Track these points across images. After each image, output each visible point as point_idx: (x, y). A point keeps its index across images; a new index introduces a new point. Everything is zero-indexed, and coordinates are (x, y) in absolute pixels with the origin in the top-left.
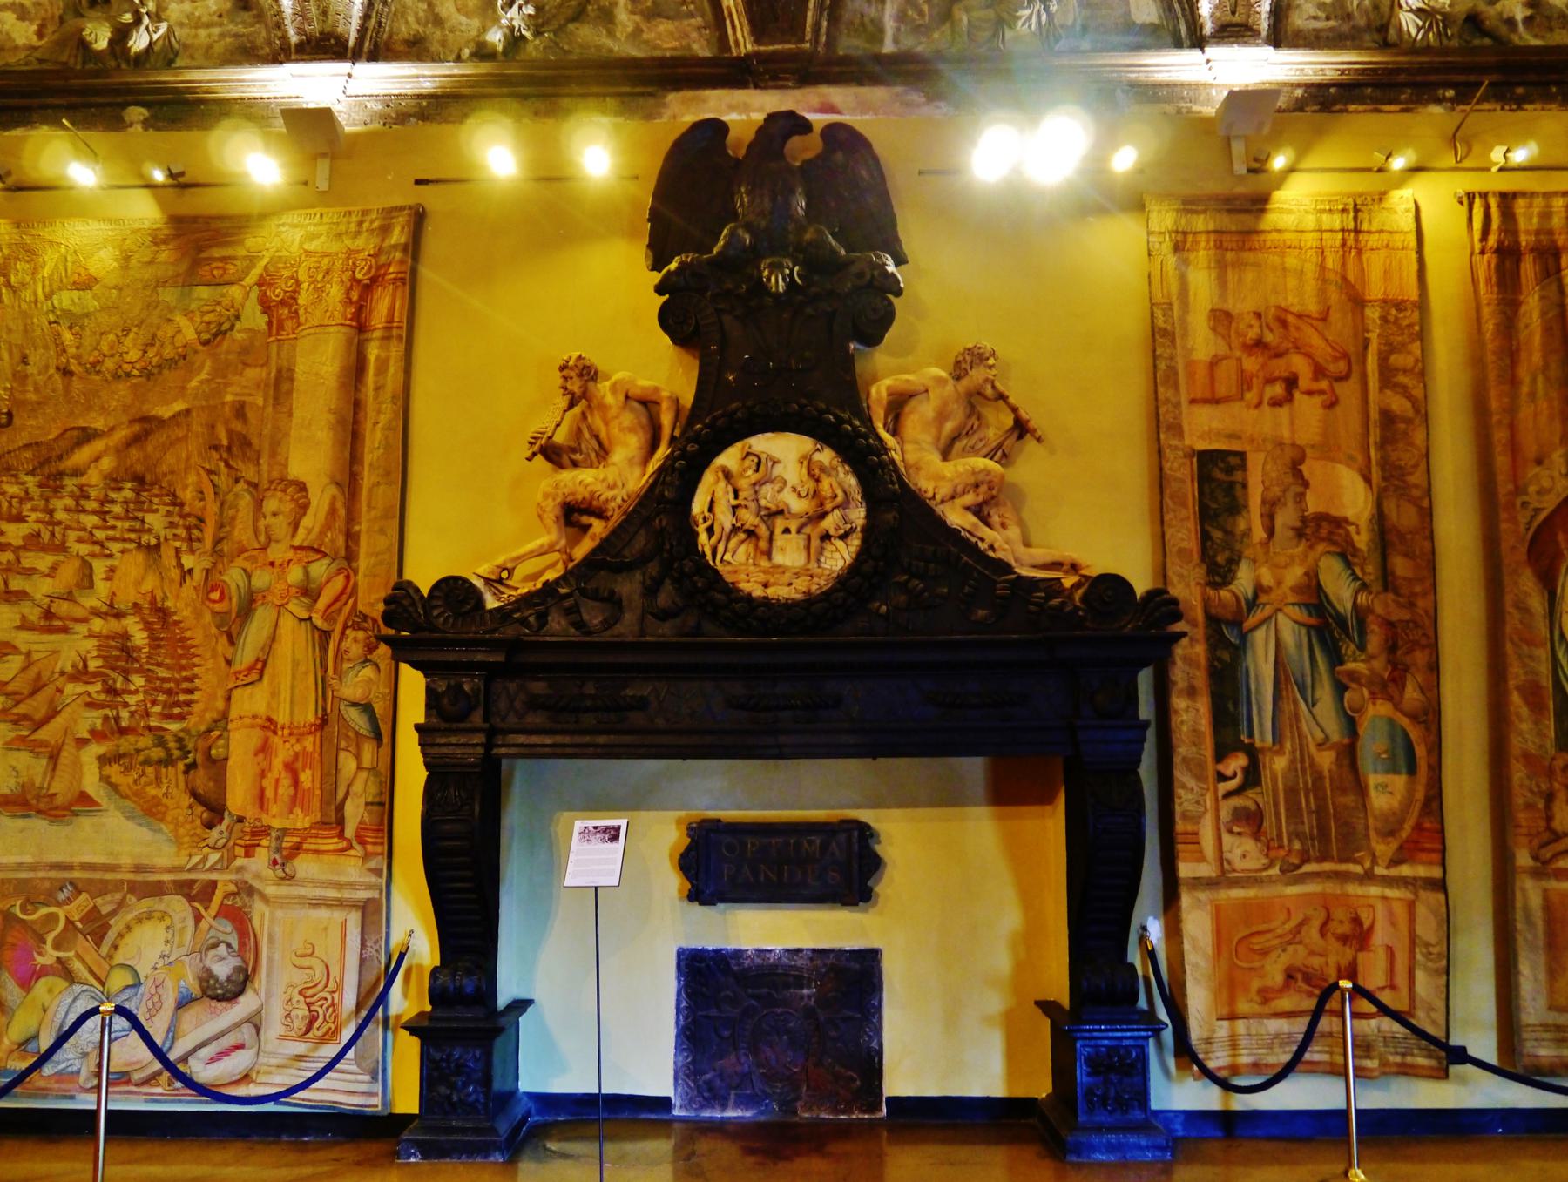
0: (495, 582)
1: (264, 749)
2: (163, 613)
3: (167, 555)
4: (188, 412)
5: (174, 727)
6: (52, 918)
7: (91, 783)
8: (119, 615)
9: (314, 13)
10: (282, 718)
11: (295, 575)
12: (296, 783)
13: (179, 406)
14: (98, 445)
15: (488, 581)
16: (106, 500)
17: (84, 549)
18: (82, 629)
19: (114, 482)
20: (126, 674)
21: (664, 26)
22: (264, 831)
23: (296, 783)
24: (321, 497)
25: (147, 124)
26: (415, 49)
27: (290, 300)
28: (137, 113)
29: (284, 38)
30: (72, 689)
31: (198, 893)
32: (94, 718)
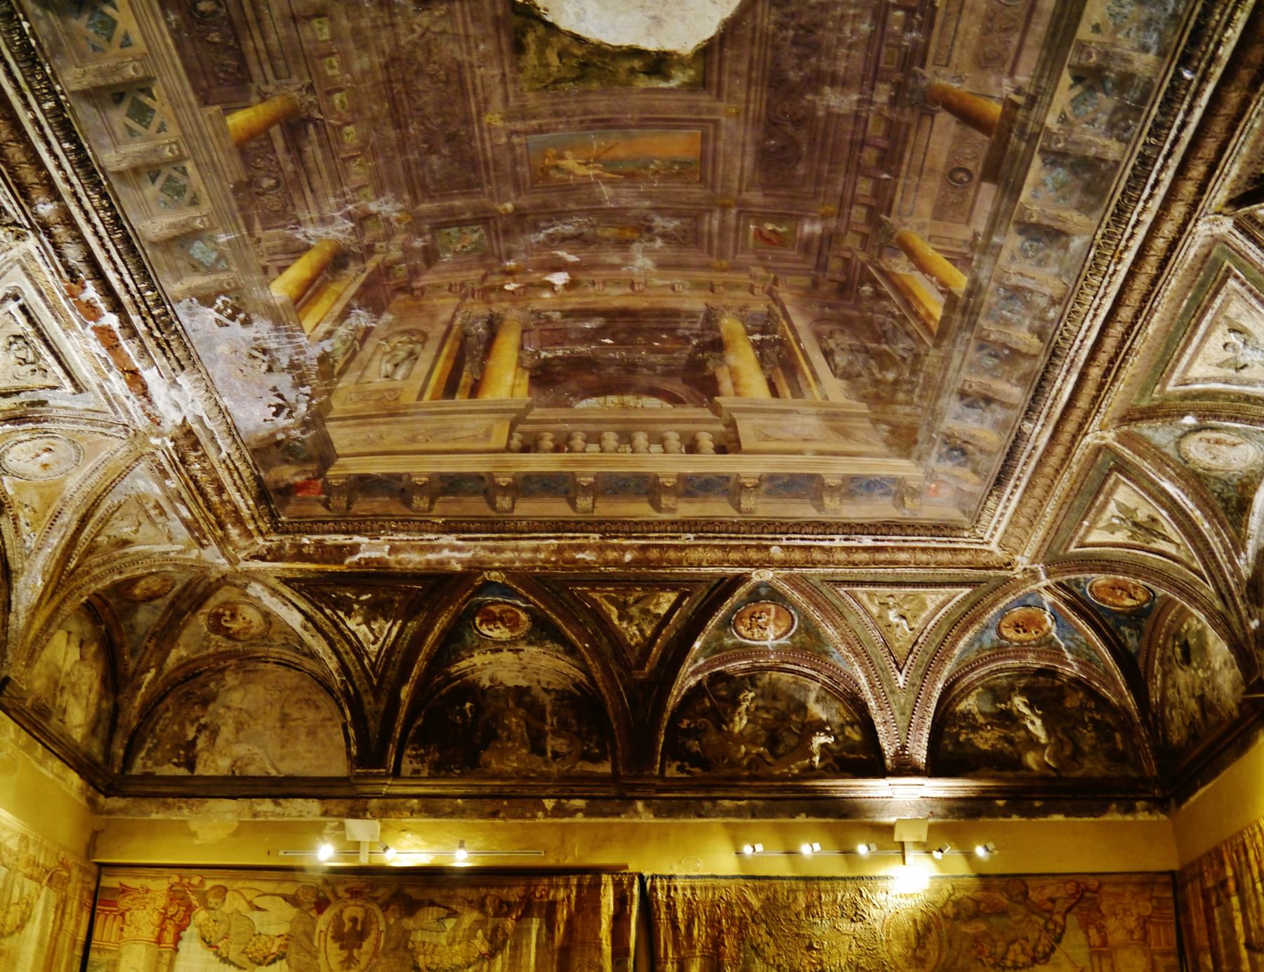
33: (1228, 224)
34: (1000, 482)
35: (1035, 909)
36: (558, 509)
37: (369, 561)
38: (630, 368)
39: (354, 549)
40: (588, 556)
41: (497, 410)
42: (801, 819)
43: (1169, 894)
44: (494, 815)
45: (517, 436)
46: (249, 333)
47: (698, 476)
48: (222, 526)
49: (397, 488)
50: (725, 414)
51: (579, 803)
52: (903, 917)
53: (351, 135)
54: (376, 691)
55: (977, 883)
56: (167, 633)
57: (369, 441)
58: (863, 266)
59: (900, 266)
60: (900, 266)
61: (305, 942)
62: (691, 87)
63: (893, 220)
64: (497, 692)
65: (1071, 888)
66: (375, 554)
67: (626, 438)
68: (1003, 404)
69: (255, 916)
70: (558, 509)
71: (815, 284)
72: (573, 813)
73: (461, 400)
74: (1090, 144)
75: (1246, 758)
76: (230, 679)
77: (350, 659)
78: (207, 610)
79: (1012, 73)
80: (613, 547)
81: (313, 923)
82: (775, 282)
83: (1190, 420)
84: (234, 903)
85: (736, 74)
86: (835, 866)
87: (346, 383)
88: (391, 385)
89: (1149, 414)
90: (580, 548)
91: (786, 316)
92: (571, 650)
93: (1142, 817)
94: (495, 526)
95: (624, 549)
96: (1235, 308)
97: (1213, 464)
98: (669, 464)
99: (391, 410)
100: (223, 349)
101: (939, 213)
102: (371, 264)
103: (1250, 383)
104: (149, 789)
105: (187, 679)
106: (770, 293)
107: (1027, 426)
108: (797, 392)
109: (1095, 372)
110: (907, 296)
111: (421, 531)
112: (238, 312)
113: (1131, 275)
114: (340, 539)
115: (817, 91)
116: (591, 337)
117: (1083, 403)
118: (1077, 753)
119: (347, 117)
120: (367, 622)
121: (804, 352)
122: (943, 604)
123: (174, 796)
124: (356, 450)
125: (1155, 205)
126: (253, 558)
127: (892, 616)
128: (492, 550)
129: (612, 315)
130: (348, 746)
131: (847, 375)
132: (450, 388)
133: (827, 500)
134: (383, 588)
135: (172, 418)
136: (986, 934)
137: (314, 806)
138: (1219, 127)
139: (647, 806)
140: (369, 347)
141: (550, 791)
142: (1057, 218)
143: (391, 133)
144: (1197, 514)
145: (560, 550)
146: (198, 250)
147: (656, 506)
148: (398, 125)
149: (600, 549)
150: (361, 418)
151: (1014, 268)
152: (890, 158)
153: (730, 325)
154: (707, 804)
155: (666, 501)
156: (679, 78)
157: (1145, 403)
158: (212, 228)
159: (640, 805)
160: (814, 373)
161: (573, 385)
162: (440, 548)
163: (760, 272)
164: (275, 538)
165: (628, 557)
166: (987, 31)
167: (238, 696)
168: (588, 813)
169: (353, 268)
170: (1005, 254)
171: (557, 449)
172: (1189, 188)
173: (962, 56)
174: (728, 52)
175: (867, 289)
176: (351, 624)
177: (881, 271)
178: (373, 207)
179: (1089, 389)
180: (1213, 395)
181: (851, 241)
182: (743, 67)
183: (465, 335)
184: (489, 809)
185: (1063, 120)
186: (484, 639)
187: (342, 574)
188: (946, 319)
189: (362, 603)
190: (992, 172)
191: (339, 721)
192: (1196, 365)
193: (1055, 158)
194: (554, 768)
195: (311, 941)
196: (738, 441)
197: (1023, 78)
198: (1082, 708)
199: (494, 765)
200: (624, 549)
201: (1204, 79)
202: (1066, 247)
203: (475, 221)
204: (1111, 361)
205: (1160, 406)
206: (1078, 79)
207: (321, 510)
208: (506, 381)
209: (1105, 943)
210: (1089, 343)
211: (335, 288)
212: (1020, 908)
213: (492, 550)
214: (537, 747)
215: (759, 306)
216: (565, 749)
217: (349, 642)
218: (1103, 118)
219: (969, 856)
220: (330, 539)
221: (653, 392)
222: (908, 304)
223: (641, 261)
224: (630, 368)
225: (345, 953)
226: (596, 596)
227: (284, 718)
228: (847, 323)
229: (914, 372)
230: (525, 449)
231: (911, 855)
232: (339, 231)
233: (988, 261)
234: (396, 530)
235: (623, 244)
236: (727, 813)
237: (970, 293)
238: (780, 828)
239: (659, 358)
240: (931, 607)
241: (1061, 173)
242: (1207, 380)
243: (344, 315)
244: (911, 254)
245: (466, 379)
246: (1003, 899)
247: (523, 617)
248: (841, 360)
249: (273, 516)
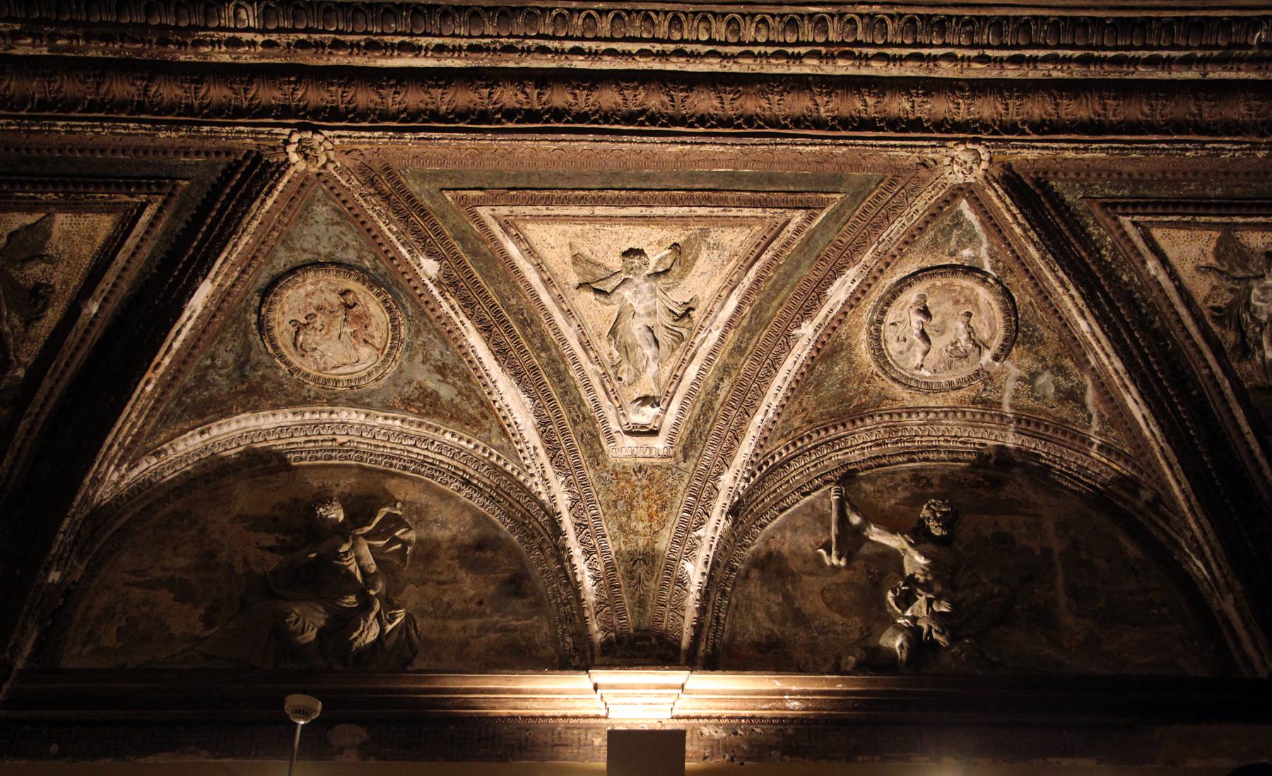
25: (365, 751)
29: (582, 634)
96: (735, 239)
117: (394, 100)
125: (978, 71)
157: (414, 187)
192: (558, 228)
204: (558, 114)
205: (423, 212)
242: (530, 252)
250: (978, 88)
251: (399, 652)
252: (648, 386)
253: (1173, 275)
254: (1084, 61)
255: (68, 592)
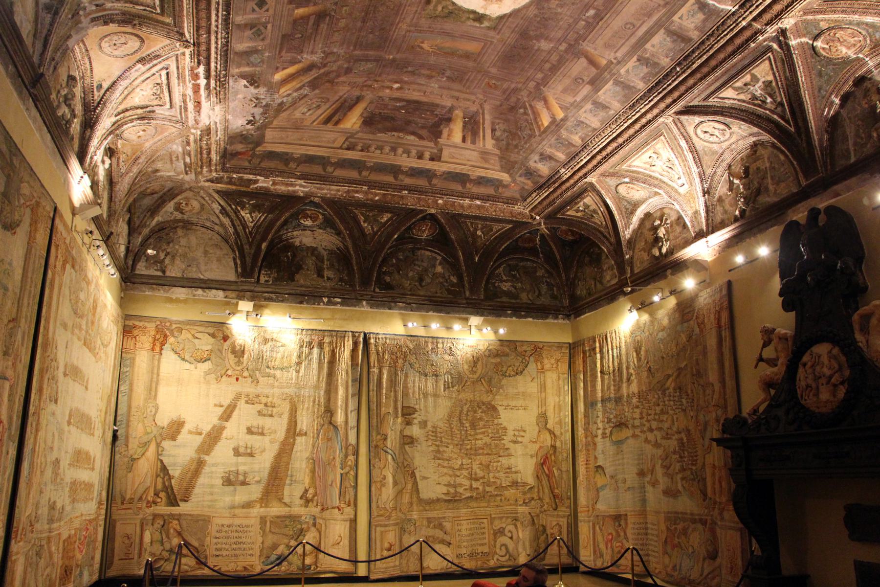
0: (755, 411)
1: (713, 475)
2: (688, 431)
3: (688, 411)
4: (686, 365)
5: (694, 468)
6: (676, 529)
7: (680, 487)
8: (680, 433)
9: (696, 223)
10: (716, 464)
11: (714, 415)
12: (721, 486)
13: (685, 363)
14: (671, 379)
15: (749, 414)
16: (674, 396)
17: (671, 412)
18: (674, 438)
19: (674, 389)
20: (683, 451)
21: (783, 185)
22: (715, 503)
23: (721, 486)
24: (717, 386)
25: (672, 274)
26: (722, 225)
27: (703, 322)
28: (669, 271)
30: (674, 457)
31: (704, 523)
32: (678, 466)
33: (671, 119)
34: (540, 187)
35: (519, 354)
36: (354, 174)
37: (261, 188)
38: (408, 123)
39: (256, 182)
40: (360, 196)
41: (343, 132)
42: (431, 313)
43: (568, 351)
44: (301, 303)
45: (347, 143)
46: (256, 91)
47: (418, 168)
48: (202, 167)
49: (285, 158)
50: (439, 146)
51: (339, 300)
52: (469, 355)
53: (342, 23)
54: (250, 244)
55: (498, 343)
56: (154, 210)
57: (282, 138)
58: (524, 102)
59: (539, 106)
60: (539, 106)
61: (219, 354)
62: (489, 28)
63: (545, 89)
64: (302, 248)
65: (532, 347)
66: (265, 185)
67: (394, 149)
68: (556, 161)
69: (196, 341)
70: (354, 174)
71: (501, 105)
72: (336, 304)
73: (329, 126)
74: (633, 81)
75: (611, 305)
76: (180, 232)
77: (240, 228)
78: (175, 200)
79: (616, 52)
80: (372, 193)
81: (222, 345)
82: (485, 101)
83: (627, 180)
84: (185, 335)
85: (510, 27)
86: (443, 334)
87: (284, 115)
88: (303, 117)
89: (612, 175)
90: (357, 192)
91: (483, 114)
92: (339, 233)
93: (561, 321)
94: (324, 179)
95: (376, 195)
97: (627, 195)
98: (407, 162)
99: (297, 127)
100: (240, 96)
101: (565, 91)
102: (322, 71)
103: (653, 171)
104: (144, 281)
105: (159, 230)
106: (481, 106)
107: (563, 170)
108: (473, 142)
109: (599, 157)
110: (536, 115)
111: (288, 178)
112: (253, 81)
113: (628, 127)
114: (251, 177)
115: (538, 40)
116: (398, 109)
117: (590, 166)
118: (540, 294)
119: (345, 16)
120: (250, 214)
121: (484, 129)
122: (500, 230)
123: (156, 284)
124: (273, 141)
126: (208, 181)
127: (479, 233)
128: (318, 188)
129: (409, 102)
130: (236, 267)
131: (497, 140)
132: (327, 121)
133: (468, 185)
134: (264, 200)
135: (204, 120)
136: (500, 363)
137: (220, 294)
138: (683, 88)
139: (368, 303)
140: (302, 102)
141: (326, 294)
142: (609, 103)
143: (359, 24)
144: (615, 212)
145: (348, 192)
146: (254, 58)
147: (396, 178)
148: (364, 21)
149: (366, 193)
150: (282, 129)
151: (584, 115)
152: (554, 69)
153: (458, 113)
154: (393, 304)
155: (401, 177)
156: (486, 24)
157: (611, 171)
158: (265, 49)
159: (364, 303)
160: (484, 136)
161: (380, 126)
162: (296, 185)
163: (481, 96)
164: (222, 174)
165: (377, 198)
166: (613, 36)
167: (184, 241)
168: (342, 304)
169: (314, 71)
170: (583, 110)
171: (362, 151)
172: (662, 105)
173: (600, 42)
174: (510, 19)
175: (522, 110)
176: (243, 213)
177: (531, 106)
178: (335, 50)
179: (594, 162)
180: (638, 173)
181: (524, 93)
182: (514, 26)
183: (345, 101)
184: (299, 300)
185: (627, 71)
186: (299, 225)
187: (248, 192)
188: (548, 127)
189: (250, 205)
190: (592, 82)
191: (232, 256)
193: (617, 83)
194: (328, 285)
195: (221, 352)
196: (440, 157)
197: (619, 55)
198: (543, 277)
199: (302, 281)
200: (376, 195)
201: (683, 73)
202: (607, 113)
203: (375, 61)
206: (638, 60)
207: (246, 164)
208: (353, 121)
209: (542, 369)
210: (601, 147)
211: (302, 78)
212: (514, 354)
213: (318, 188)
214: (320, 274)
215: (474, 108)
216: (332, 276)
217: (240, 221)
218: (642, 75)
219: (496, 332)
220: (246, 177)
221: (413, 133)
222: (535, 119)
223: (434, 85)
224: (408, 123)
225: (237, 359)
226: (357, 212)
227: (206, 253)
228: (506, 121)
229: (525, 143)
230: (348, 149)
231: (474, 330)
232: (316, 58)
233: (575, 110)
234: (277, 176)
235: (430, 77)
236: (400, 308)
237: (562, 120)
238: (423, 317)
239: (423, 121)
240: (494, 230)
241: (618, 89)
243: (300, 88)
244: (546, 101)
245: (336, 118)
246: (507, 350)
247: (321, 217)
248: (498, 133)
249: (224, 164)
250: (651, 108)
251: (671, 252)
252: (677, 177)
253: (734, 99)
254: (659, 94)
255: (632, 258)
